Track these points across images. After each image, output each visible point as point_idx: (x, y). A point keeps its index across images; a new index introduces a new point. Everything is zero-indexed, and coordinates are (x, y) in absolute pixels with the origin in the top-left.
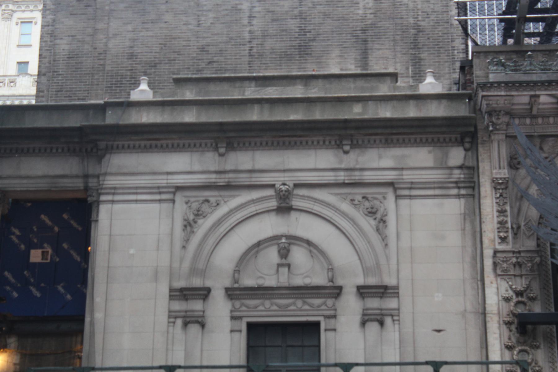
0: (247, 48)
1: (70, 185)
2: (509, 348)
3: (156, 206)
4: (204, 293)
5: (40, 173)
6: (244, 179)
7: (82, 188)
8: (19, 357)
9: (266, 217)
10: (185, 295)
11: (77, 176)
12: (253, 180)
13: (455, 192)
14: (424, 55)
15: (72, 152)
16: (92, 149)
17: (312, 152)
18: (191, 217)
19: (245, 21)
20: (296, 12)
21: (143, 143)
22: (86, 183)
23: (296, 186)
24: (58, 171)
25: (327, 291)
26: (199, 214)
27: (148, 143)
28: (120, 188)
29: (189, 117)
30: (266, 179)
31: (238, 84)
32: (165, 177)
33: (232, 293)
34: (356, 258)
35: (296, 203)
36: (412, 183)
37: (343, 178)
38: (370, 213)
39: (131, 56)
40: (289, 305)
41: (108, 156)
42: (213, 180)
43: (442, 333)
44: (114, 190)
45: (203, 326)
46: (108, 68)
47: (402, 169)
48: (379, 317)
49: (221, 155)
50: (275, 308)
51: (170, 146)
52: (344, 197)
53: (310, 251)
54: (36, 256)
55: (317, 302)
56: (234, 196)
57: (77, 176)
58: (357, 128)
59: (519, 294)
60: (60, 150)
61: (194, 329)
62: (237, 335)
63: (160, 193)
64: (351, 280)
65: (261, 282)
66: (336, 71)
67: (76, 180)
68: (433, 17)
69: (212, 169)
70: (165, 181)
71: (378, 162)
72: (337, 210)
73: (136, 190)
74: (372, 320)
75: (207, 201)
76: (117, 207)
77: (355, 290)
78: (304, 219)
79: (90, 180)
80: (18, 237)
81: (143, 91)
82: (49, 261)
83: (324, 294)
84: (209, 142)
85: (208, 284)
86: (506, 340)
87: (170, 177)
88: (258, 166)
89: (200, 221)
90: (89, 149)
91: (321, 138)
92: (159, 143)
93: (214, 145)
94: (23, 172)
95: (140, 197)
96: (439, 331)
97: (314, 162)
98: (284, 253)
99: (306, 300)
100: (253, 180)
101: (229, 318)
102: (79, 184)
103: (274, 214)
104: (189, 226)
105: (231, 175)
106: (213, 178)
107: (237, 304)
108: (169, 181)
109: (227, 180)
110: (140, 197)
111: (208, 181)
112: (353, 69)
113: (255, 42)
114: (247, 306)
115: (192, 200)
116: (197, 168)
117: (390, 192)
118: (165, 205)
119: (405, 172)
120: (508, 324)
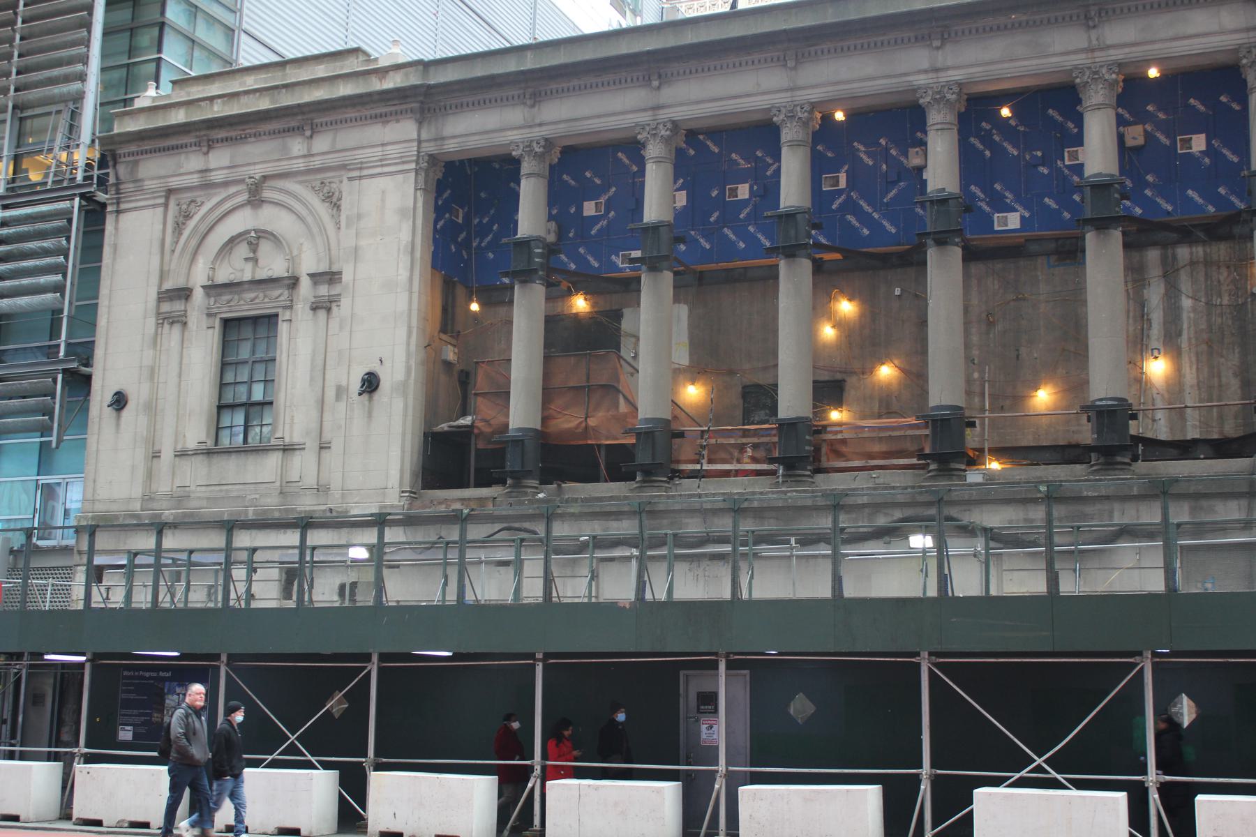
93: (1082, 17)
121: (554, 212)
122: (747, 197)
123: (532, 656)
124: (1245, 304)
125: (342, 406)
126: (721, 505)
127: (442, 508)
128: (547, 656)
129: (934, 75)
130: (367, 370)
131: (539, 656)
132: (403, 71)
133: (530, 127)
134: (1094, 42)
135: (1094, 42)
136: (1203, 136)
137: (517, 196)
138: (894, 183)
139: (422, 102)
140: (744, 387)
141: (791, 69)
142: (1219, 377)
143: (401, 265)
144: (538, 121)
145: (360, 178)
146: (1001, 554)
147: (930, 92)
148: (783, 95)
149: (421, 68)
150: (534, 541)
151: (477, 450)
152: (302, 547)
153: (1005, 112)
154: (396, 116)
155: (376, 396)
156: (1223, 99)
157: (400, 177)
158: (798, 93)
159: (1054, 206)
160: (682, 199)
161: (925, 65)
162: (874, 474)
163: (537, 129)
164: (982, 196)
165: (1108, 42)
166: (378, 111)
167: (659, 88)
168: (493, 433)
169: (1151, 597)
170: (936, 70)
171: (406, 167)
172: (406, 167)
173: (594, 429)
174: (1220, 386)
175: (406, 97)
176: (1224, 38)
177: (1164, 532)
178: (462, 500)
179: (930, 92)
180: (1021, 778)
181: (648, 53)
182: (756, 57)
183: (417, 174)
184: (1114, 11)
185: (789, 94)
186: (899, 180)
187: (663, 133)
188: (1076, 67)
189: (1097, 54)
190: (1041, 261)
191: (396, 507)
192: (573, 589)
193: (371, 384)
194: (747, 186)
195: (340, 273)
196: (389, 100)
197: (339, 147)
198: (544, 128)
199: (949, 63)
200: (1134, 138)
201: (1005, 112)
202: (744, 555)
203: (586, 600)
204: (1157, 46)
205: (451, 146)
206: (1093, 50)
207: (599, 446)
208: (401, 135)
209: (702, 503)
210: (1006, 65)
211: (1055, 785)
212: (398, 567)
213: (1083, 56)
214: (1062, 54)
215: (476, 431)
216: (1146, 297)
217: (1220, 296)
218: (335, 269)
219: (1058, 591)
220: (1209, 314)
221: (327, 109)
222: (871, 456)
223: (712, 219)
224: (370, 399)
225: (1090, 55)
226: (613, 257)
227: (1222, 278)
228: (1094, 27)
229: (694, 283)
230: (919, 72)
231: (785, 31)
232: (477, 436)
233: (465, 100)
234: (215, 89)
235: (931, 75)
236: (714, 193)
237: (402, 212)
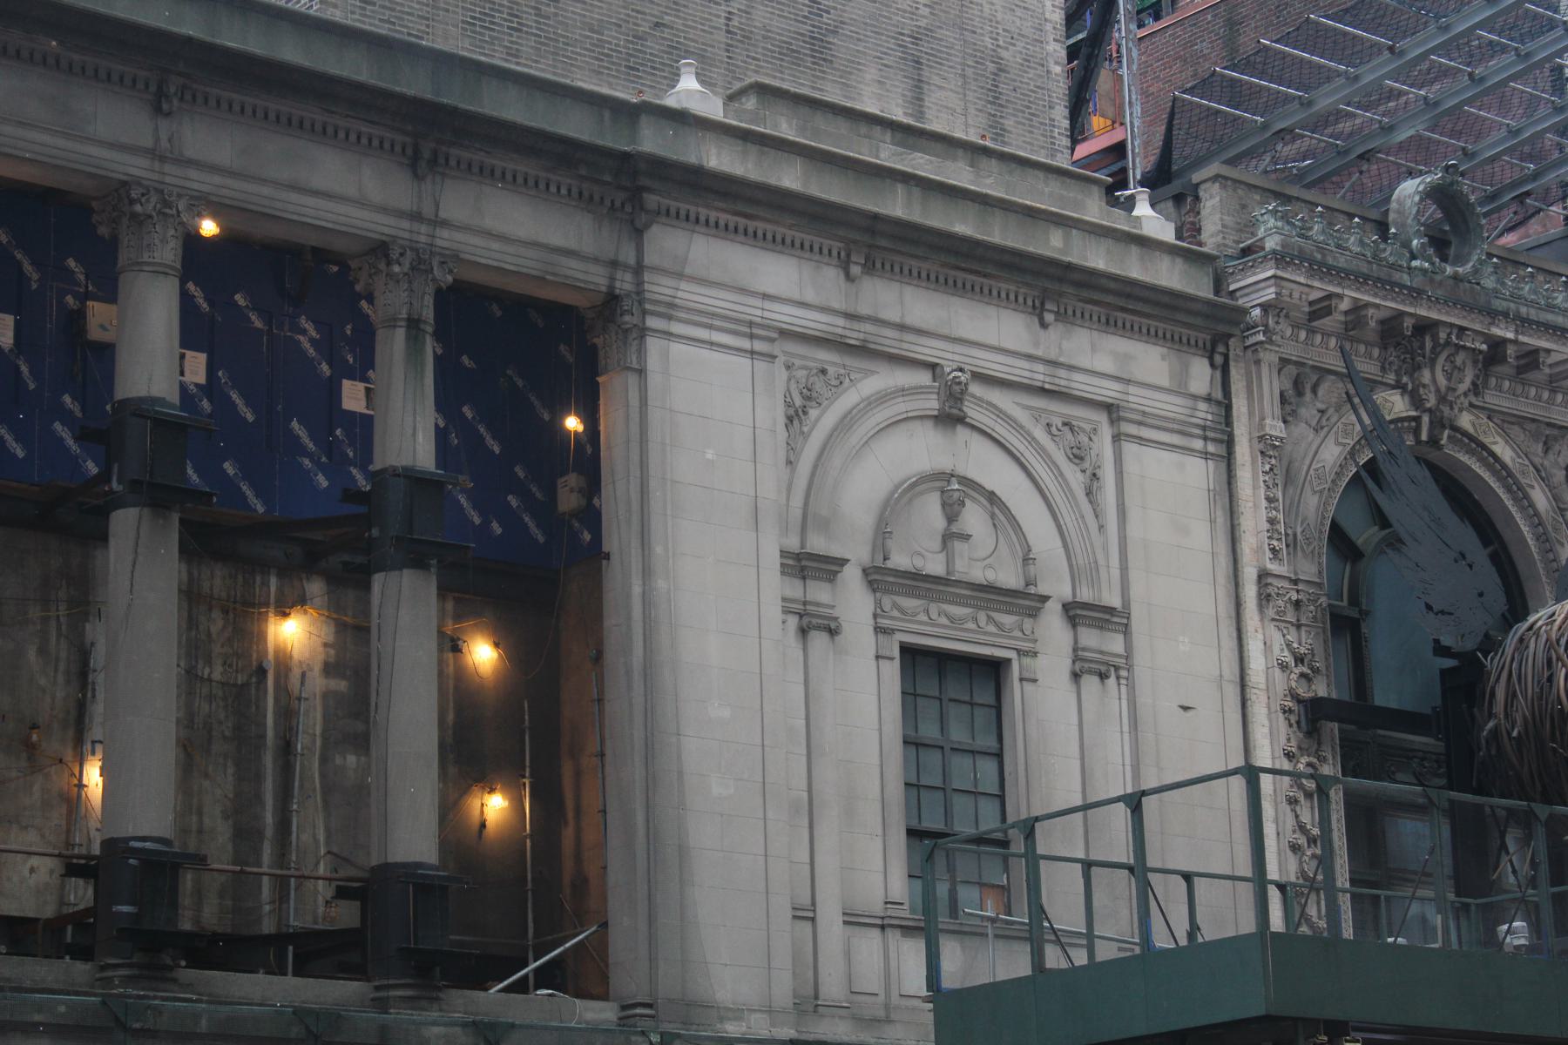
1: (581, 276)
2: (1289, 756)
3: (744, 362)
5: (522, 233)
6: (888, 340)
7: (604, 289)
8: (332, 629)
9: (917, 424)
10: (803, 569)
11: (596, 260)
12: (905, 346)
13: (1198, 444)
14: (1009, 123)
15: (585, 201)
16: (623, 205)
17: (992, 311)
18: (798, 402)
21: (724, 218)
22: (612, 279)
23: (979, 377)
24: (557, 240)
25: (1027, 603)
26: (809, 396)
27: (733, 220)
28: (689, 310)
29: (790, 177)
30: (928, 350)
31: (863, 129)
32: (758, 302)
33: (879, 578)
34: (1059, 543)
35: (973, 413)
36: (1144, 413)
37: (1041, 377)
38: (1075, 456)
40: (963, 620)
41: (655, 229)
42: (839, 331)
43: (1190, 713)
44: (670, 310)
47: (1128, 382)
48: (1103, 669)
49: (849, 277)
50: (944, 621)
51: (741, 229)
52: (1037, 414)
53: (993, 516)
55: (1007, 620)
56: (868, 373)
57: (596, 260)
58: (1079, 285)
59: (1299, 660)
60: (564, 191)
61: (819, 640)
62: (884, 664)
63: (752, 337)
64: (1059, 587)
65: (919, 563)
66: (872, 108)
67: (593, 268)
68: (1020, 45)
69: (836, 305)
70: (759, 313)
71: (1101, 357)
72: (1031, 440)
73: (709, 319)
74: (1090, 672)
75: (824, 372)
76: (677, 348)
77: (1060, 607)
78: (978, 445)
79: (619, 275)
80: (312, 340)
81: (688, 90)
83: (958, 595)
85: (836, 551)
86: (1283, 740)
87: (768, 305)
88: (909, 321)
89: (813, 413)
90: (618, 204)
91: (1013, 288)
92: (752, 225)
94: (488, 223)
95: (718, 337)
96: (1185, 708)
97: (992, 331)
98: (952, 511)
99: (994, 614)
100: (905, 346)
102: (597, 278)
103: (929, 424)
104: (794, 418)
105: (868, 327)
107: (887, 602)
108: (766, 314)
109: (862, 336)
110: (718, 337)
111: (831, 329)
112: (898, 114)
114: (996, 624)
115: (798, 362)
116: (810, 296)
117: (1102, 418)
118: (761, 365)
119: (1132, 389)
120: (1286, 711)
124: (246, 685)
134: (164, 144)
135: (164, 144)
136: (202, 358)
142: (200, 814)
158: (445, 233)
165: (189, 153)
174: (200, 831)
176: (365, 214)
188: (138, 182)
189: (167, 168)
194: (580, 428)
200: (103, 327)
204: (266, 191)
206: (162, 159)
213: (143, 162)
214: (112, 146)
216: (89, 637)
225: (157, 165)
227: (214, 630)
228: (168, 114)
234: (959, 174)
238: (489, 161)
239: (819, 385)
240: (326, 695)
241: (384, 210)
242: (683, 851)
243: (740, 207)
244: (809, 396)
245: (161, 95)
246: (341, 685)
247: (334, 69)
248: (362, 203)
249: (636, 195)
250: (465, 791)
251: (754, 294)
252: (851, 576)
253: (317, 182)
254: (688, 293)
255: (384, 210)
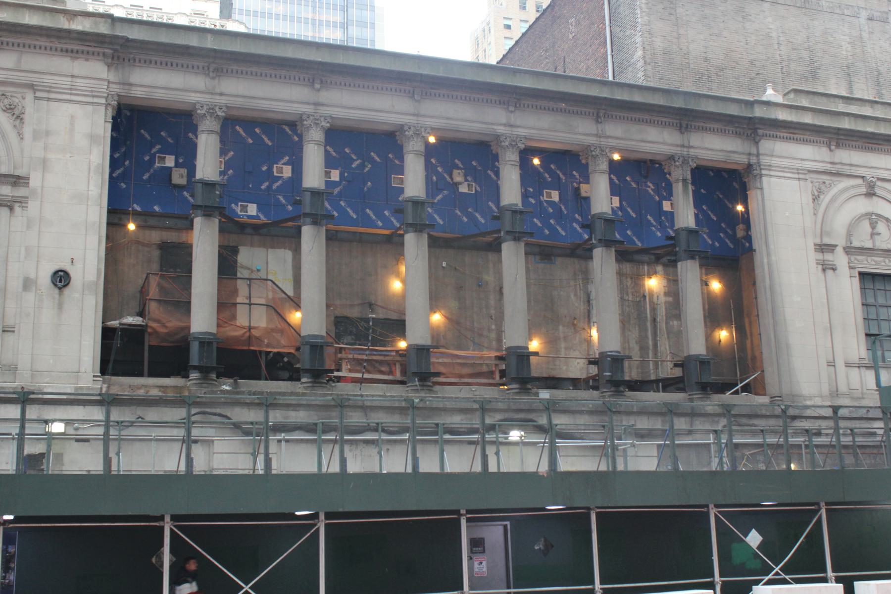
0: (779, 66)
3: (797, 182)
4: (831, 248)
5: (718, 147)
6: (846, 170)
9: (859, 197)
11: (743, 154)
14: (883, 92)
15: (737, 134)
17: (882, 156)
18: (816, 193)
19: (776, 46)
20: (806, 45)
23: (879, 179)
24: (730, 148)
26: (820, 191)
27: (789, 135)
29: (808, 119)
30: (860, 172)
31: (832, 100)
33: (849, 250)
35: (878, 191)
39: (706, 60)
40: (880, 262)
44: (769, 167)
45: (834, 270)
46: (692, 66)
49: (831, 150)
54: (555, 196)
57: (743, 154)
61: (830, 273)
63: (798, 173)
67: (742, 156)
76: (773, 180)
81: (770, 94)
82: (275, 174)
84: (825, 140)
88: (853, 163)
89: (822, 197)
92: (795, 136)
94: (707, 145)
98: (873, 226)
101: (847, 268)
102: (744, 159)
103: (863, 197)
104: (815, 199)
105: (839, 166)
106: (828, 167)
107: (853, 258)
113: (784, 64)
116: (818, 158)
118: (802, 183)
121: (181, 161)
122: (337, 179)
123: (457, 512)
124: (640, 301)
125: (30, 297)
126: (333, 403)
127: (142, 392)
128: (468, 512)
129: (510, 129)
130: (57, 268)
131: (463, 512)
132: (94, 19)
133: (212, 94)
136: (617, 198)
137: (195, 146)
138: (440, 190)
139: (116, 50)
140: (336, 317)
141: (417, 101)
143: (92, 182)
144: (218, 91)
145: (49, 99)
146: (213, 441)
147: (205, 108)
148: (411, 118)
149: (109, 21)
150: (227, 423)
151: (150, 346)
152: (23, 421)
153: (536, 161)
154: (88, 55)
155: (67, 291)
156: (347, 150)
157: (90, 108)
158: (692, 150)
159: (539, 224)
160: (335, 175)
161: (504, 121)
162: (474, 388)
163: (218, 97)
164: (654, 223)
165: (608, 134)
166: (70, 47)
167: (319, 90)
168: (168, 334)
169: (437, 473)
170: (511, 126)
171: (96, 100)
172: (96, 100)
173: (257, 338)
175: (103, 43)
177: (670, 433)
178: (159, 387)
179: (205, 108)
180: (769, 580)
181: (320, 63)
182: (394, 86)
183: (106, 109)
184: (177, 65)
185: (415, 118)
186: (443, 190)
187: (323, 124)
189: (602, 139)
190: (559, 260)
191: (93, 389)
192: (429, 464)
193: (61, 279)
195: (28, 178)
196: (85, 40)
197: (24, 67)
198: (223, 97)
199: (518, 123)
201: (536, 161)
202: (493, 443)
203: (251, 472)
204: (633, 143)
205: (138, 92)
206: (600, 137)
207: (260, 352)
208: (94, 72)
209: (363, 401)
210: (552, 133)
211: (784, 582)
212: (87, 440)
213: (595, 139)
215: (149, 330)
217: (627, 295)
218: (18, 172)
219: (346, 471)
220: (622, 305)
221: (21, 33)
222: (461, 376)
223: (263, 187)
224: (61, 294)
226: (233, 205)
229: (542, 253)
230: (501, 124)
231: (421, 75)
232: (150, 334)
233: (154, 58)
234: (867, 111)
235: (507, 128)
236: (264, 168)
237: (93, 138)
238: (705, 125)
239: (823, 187)
240: (666, 302)
241: (672, 145)
242: (788, 346)
243: (791, 131)
244: (820, 191)
245: (598, 116)
246: (670, 299)
247: (652, 102)
248: (664, 143)
249: (755, 130)
250: (713, 331)
251: (797, 159)
252: (839, 250)
253: (650, 138)
254: (775, 161)
255: (672, 145)
